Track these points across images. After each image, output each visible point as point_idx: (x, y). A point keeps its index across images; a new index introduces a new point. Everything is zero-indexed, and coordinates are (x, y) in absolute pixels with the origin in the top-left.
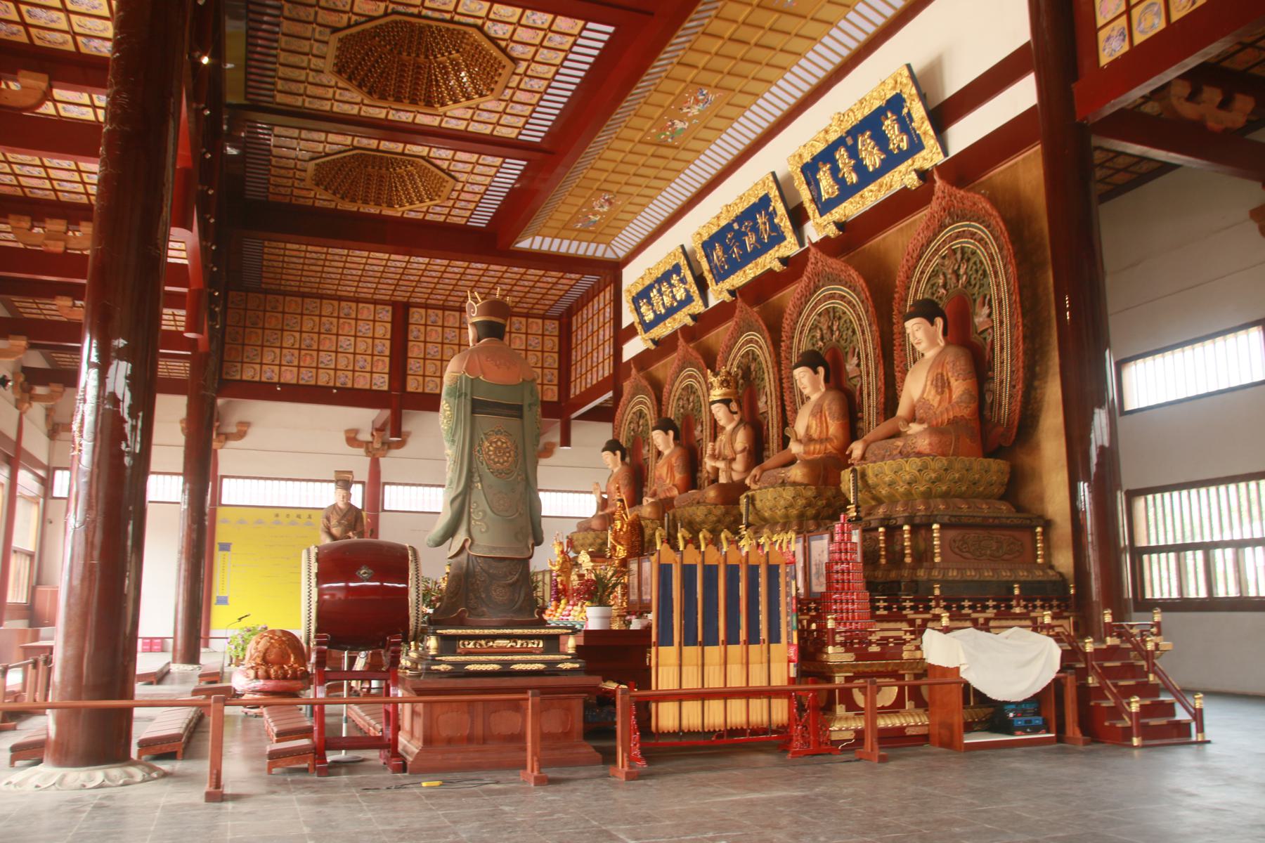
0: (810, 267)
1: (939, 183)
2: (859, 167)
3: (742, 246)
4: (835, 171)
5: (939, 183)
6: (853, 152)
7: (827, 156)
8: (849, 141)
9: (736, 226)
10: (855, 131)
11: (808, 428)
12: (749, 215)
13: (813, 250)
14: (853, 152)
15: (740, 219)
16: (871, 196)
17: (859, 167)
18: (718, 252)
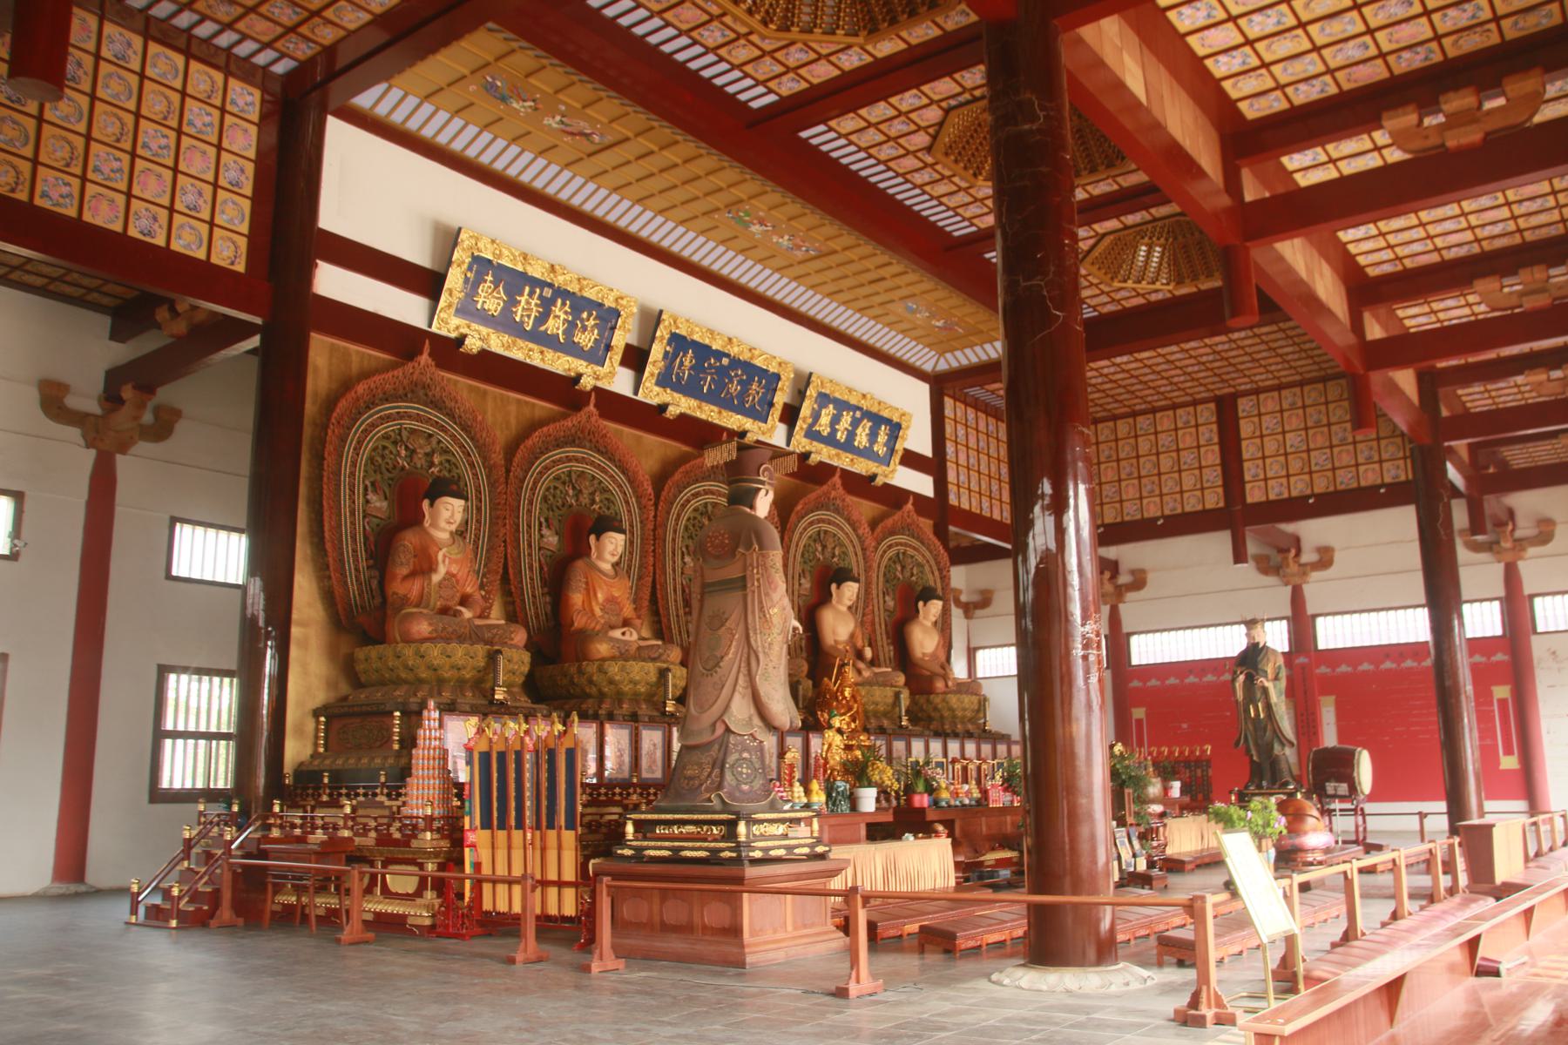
0: (825, 487)
1: (909, 506)
2: (851, 434)
3: (721, 385)
4: (835, 420)
5: (909, 506)
6: (856, 423)
7: (842, 406)
8: (858, 414)
9: (725, 361)
10: (869, 415)
11: (852, 636)
12: (750, 370)
13: (837, 479)
14: (856, 423)
15: (736, 363)
16: (844, 461)
17: (851, 434)
18: (688, 360)
